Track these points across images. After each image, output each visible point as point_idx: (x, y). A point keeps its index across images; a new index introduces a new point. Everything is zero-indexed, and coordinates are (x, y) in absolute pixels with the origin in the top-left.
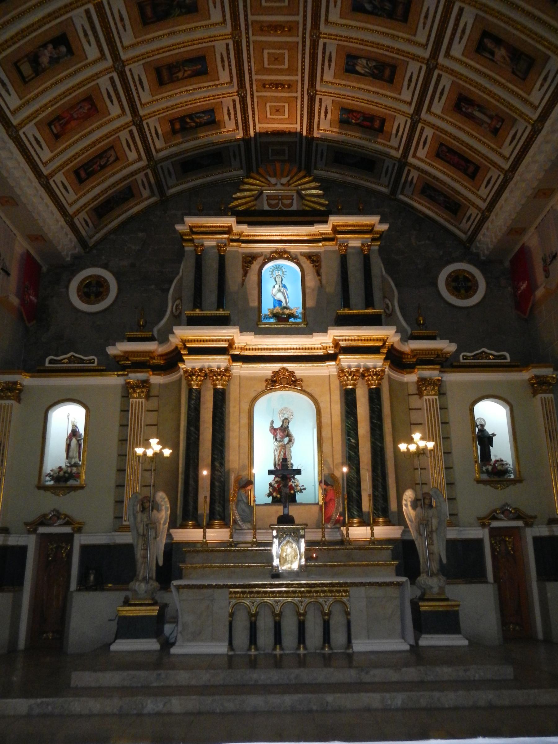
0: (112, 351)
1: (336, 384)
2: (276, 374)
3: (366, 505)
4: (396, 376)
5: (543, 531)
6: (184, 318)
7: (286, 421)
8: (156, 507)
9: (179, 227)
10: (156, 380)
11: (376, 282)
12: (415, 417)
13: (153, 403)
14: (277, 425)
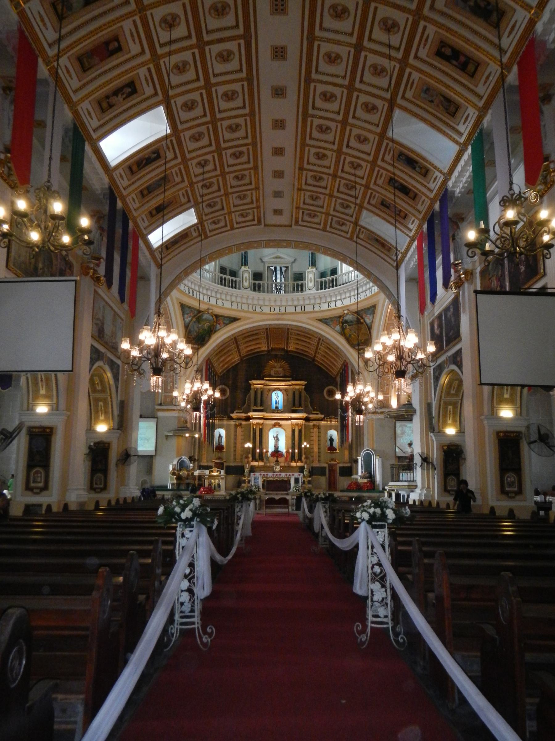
0: (231, 415)
1: (290, 427)
2: (275, 423)
3: (296, 458)
4: (307, 423)
5: (341, 465)
6: (252, 410)
7: (277, 435)
8: (249, 458)
9: (250, 382)
10: (244, 423)
11: (303, 399)
12: (312, 434)
13: (243, 429)
14: (275, 436)
